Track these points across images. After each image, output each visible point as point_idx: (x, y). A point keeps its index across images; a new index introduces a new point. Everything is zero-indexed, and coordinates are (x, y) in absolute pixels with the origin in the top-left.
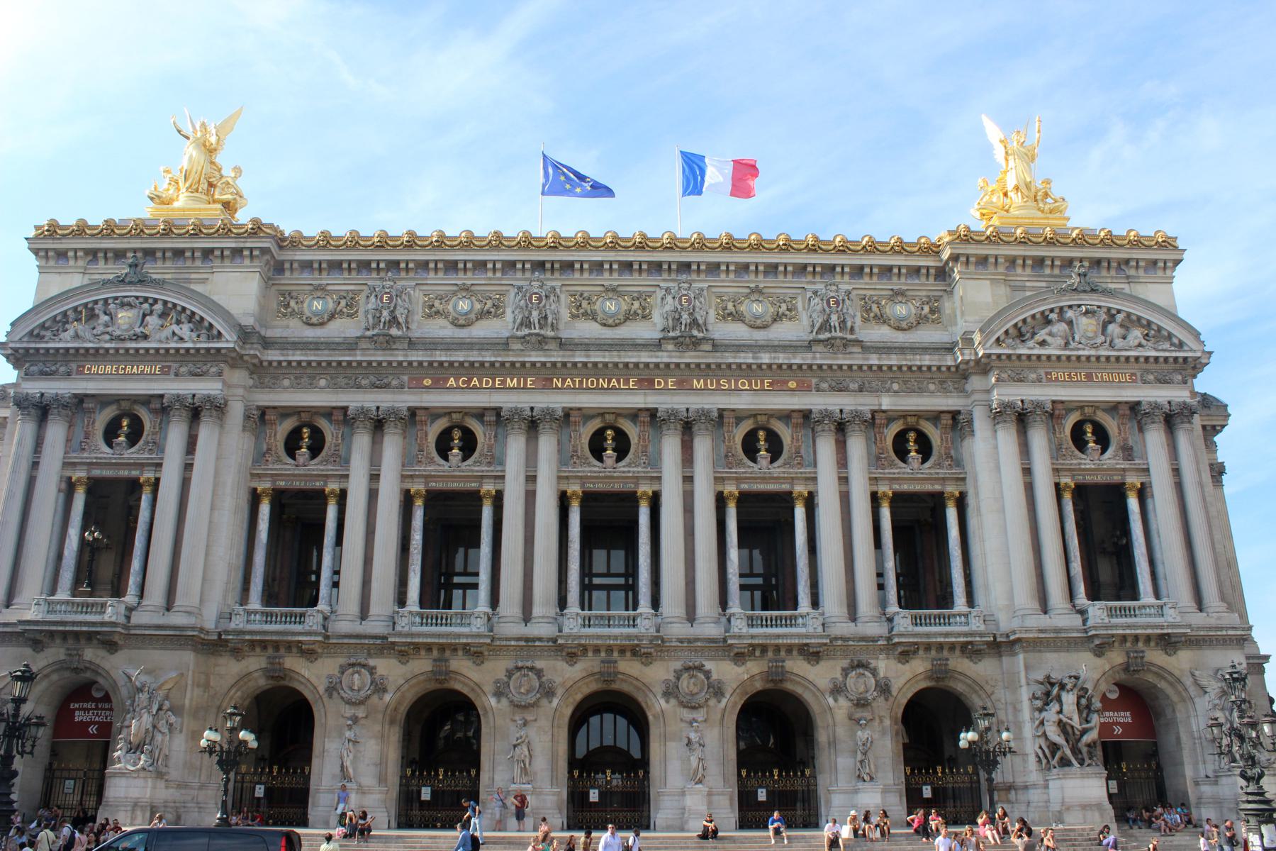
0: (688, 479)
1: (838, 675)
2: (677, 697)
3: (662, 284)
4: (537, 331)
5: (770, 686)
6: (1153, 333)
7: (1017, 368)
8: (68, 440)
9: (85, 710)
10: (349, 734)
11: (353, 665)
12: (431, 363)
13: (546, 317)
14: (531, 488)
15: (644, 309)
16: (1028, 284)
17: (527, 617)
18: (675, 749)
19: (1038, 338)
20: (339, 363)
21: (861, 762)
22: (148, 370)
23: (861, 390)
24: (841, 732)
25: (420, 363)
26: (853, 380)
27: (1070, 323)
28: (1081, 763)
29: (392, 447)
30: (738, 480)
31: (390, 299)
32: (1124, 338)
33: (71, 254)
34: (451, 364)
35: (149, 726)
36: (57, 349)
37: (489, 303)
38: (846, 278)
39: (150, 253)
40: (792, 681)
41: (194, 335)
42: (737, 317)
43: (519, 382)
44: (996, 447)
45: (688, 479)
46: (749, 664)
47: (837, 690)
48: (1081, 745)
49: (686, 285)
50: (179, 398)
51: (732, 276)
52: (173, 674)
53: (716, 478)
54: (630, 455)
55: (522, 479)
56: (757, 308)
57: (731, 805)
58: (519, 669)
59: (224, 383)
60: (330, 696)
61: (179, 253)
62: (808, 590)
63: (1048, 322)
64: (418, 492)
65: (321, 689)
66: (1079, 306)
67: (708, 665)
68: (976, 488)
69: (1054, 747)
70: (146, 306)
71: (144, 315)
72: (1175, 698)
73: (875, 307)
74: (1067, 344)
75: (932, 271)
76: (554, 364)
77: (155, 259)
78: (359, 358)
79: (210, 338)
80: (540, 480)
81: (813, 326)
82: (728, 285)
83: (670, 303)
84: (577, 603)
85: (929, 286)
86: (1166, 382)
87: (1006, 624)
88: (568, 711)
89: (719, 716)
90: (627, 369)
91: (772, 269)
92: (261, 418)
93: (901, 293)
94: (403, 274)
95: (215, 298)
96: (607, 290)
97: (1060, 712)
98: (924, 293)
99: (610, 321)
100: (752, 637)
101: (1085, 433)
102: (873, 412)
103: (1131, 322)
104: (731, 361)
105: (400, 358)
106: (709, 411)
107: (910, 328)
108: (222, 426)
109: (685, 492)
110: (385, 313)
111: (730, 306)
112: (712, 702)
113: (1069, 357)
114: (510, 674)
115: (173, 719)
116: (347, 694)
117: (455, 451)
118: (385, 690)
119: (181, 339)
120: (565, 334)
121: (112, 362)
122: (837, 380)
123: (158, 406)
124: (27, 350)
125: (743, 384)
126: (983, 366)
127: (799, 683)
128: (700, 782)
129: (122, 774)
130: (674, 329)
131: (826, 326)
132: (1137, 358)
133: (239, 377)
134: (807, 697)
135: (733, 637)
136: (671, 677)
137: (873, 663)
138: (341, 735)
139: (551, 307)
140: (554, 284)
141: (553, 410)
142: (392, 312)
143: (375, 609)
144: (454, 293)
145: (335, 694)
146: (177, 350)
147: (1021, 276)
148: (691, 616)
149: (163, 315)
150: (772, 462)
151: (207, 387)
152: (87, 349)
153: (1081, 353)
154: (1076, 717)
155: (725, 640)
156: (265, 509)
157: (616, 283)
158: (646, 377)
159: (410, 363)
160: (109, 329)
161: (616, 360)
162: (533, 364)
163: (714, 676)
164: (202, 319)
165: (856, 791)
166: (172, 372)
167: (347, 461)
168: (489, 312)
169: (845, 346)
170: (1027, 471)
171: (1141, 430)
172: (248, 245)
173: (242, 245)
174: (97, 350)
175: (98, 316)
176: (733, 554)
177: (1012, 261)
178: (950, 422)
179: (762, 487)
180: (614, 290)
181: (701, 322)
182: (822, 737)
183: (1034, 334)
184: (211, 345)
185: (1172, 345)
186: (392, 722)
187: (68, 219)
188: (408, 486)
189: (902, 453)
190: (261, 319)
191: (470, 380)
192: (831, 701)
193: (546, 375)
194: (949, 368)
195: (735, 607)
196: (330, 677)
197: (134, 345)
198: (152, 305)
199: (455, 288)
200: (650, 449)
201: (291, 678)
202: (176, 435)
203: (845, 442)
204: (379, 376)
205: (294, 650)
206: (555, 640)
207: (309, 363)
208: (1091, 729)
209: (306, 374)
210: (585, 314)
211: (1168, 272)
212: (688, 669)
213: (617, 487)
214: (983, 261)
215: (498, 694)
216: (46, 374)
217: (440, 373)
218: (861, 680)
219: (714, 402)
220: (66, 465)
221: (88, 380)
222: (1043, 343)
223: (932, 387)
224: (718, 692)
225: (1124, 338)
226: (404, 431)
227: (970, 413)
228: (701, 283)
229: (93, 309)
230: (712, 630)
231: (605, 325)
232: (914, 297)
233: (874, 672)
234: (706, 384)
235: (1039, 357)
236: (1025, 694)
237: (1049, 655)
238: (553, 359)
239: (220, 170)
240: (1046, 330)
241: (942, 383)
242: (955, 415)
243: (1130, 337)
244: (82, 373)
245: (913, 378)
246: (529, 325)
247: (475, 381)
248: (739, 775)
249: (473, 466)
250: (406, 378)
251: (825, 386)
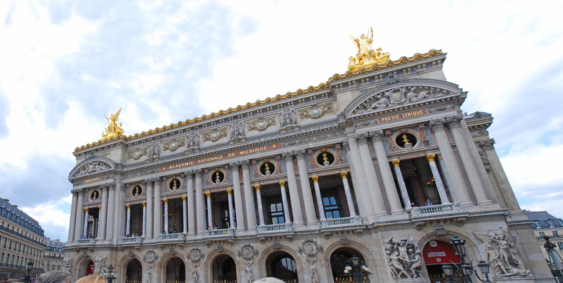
48: (412, 269)
126: (350, 123)
177: (359, 81)
249: (180, 190)
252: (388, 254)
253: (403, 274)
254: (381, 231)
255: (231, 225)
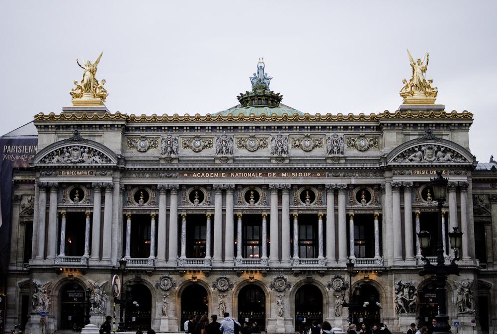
0: (280, 210)
1: (330, 280)
2: (274, 288)
3: (271, 134)
4: (225, 155)
5: (307, 283)
6: (456, 155)
7: (402, 169)
8: (58, 199)
9: (72, 293)
10: (165, 301)
11: (164, 277)
12: (187, 168)
13: (228, 150)
14: (224, 213)
15: (265, 144)
16: (411, 133)
17: (223, 260)
18: (274, 305)
19: (410, 158)
20: (153, 169)
21: (336, 310)
22: (85, 173)
23: (344, 176)
24: (331, 300)
25: (183, 168)
26: (341, 172)
27: (423, 152)
28: (408, 312)
29: (174, 199)
30: (299, 210)
31: (171, 143)
32: (444, 157)
33: (50, 127)
34: (194, 168)
35: (100, 299)
36: (52, 166)
37: (207, 143)
38: (342, 131)
39: (79, 126)
40: (315, 282)
41: (101, 160)
42: (299, 146)
43: (219, 175)
44: (392, 199)
45: (280, 210)
46: (299, 277)
47: (330, 286)
49: (280, 136)
50: (98, 184)
51: (298, 131)
52: (105, 282)
53: (290, 210)
54: (259, 201)
55: (221, 210)
56: (307, 143)
57: (293, 323)
58: (221, 278)
59: (113, 178)
60: (157, 288)
61: (90, 126)
62: (322, 250)
63: (416, 152)
64: (184, 215)
65: (154, 286)
66: (427, 145)
67: (285, 277)
68: (385, 213)
69: (400, 306)
70: (82, 149)
71: (82, 153)
72: (448, 290)
73: (352, 142)
74: (421, 160)
75: (375, 127)
76: (231, 168)
77: (82, 128)
78: (161, 167)
79: (107, 161)
80: (227, 211)
81: (328, 151)
82: (296, 134)
83: (274, 144)
84: (241, 255)
85: (375, 133)
86: (458, 174)
87: (390, 264)
88: (238, 292)
89: (289, 294)
90: (257, 170)
91: (313, 128)
92: (125, 189)
93: (363, 136)
94: (174, 132)
95: (105, 144)
96: (251, 137)
97: (403, 295)
98: (372, 136)
99: (252, 150)
100: (300, 268)
101: (428, 192)
102: (348, 185)
103: (446, 151)
104: (296, 167)
105: (176, 167)
106: (288, 185)
107: (365, 151)
108: (113, 193)
109: (279, 214)
110: (169, 149)
111: (297, 142)
112: (287, 289)
113: (421, 165)
114: (218, 280)
115: (107, 296)
116: (163, 287)
117: (196, 200)
118: (176, 286)
119: (96, 162)
120: (235, 155)
121: (72, 170)
122: (335, 172)
123: (89, 186)
124: (41, 166)
125: (300, 175)
126: (389, 168)
127: (317, 283)
128: (281, 316)
129: (94, 315)
130: (275, 153)
131: (332, 152)
132: (447, 165)
133: (117, 175)
134: (320, 288)
135: (294, 268)
136: (273, 281)
137: (343, 276)
138: (161, 301)
139: (230, 146)
140: (231, 134)
141: (232, 185)
142: (171, 148)
143: (170, 258)
144: (194, 138)
145: (159, 287)
146: (95, 166)
147: (408, 130)
148: (280, 260)
149: (89, 152)
150: (311, 203)
151: (108, 180)
152: (62, 166)
153: (425, 164)
154: (408, 297)
155: (291, 268)
156: (129, 222)
157: (254, 134)
158: (265, 172)
159: (179, 168)
160: (70, 158)
161: (254, 167)
162: (224, 168)
163: (288, 281)
164: (103, 154)
165: (335, 320)
166: (94, 174)
167: (158, 204)
168: (207, 146)
169: (339, 160)
170: (402, 208)
171: (448, 192)
172: (117, 123)
173: (114, 123)
174: (66, 166)
175: (65, 153)
176: (296, 237)
177: (405, 125)
178: (377, 188)
179: (307, 212)
180: (253, 137)
181: (285, 151)
182: (325, 301)
183: (409, 156)
184: (108, 165)
185: (462, 159)
186: (178, 296)
187: (47, 113)
188: (180, 213)
189: (359, 199)
190: (123, 150)
191: (201, 174)
192: (327, 289)
193: (229, 172)
194: (377, 168)
195: (296, 257)
196: (157, 281)
197: (80, 165)
198: (84, 149)
199: (194, 136)
200: (267, 198)
201: (143, 282)
202: (97, 197)
203: (337, 195)
204: (168, 173)
205: (144, 272)
206: (233, 268)
207: (142, 169)
208: (413, 300)
209: (141, 172)
210: (243, 146)
211: (467, 128)
212: (278, 278)
213: (255, 213)
214: (393, 125)
215: (214, 286)
216: (48, 175)
217: (190, 172)
218: (338, 282)
219: (289, 182)
220: (58, 208)
221: (63, 177)
222: (411, 160)
223: (371, 175)
224: (289, 286)
225: (444, 157)
226: (178, 193)
227: (384, 185)
228: (286, 134)
229: (62, 150)
230: (287, 265)
231: (250, 151)
232: (368, 137)
233: (343, 279)
234: (287, 175)
235: (409, 165)
236: (394, 289)
237: (403, 275)
238: (231, 167)
239: (97, 81)
240: (413, 155)
241: (375, 173)
242: (379, 185)
243: (446, 158)
244: (61, 174)
245: (363, 172)
246: (222, 153)
247: (203, 174)
248: (296, 314)
250: (178, 173)
251: (330, 175)
252: (396, 294)
253: (403, 310)
254: (395, 274)
255: (263, 254)
